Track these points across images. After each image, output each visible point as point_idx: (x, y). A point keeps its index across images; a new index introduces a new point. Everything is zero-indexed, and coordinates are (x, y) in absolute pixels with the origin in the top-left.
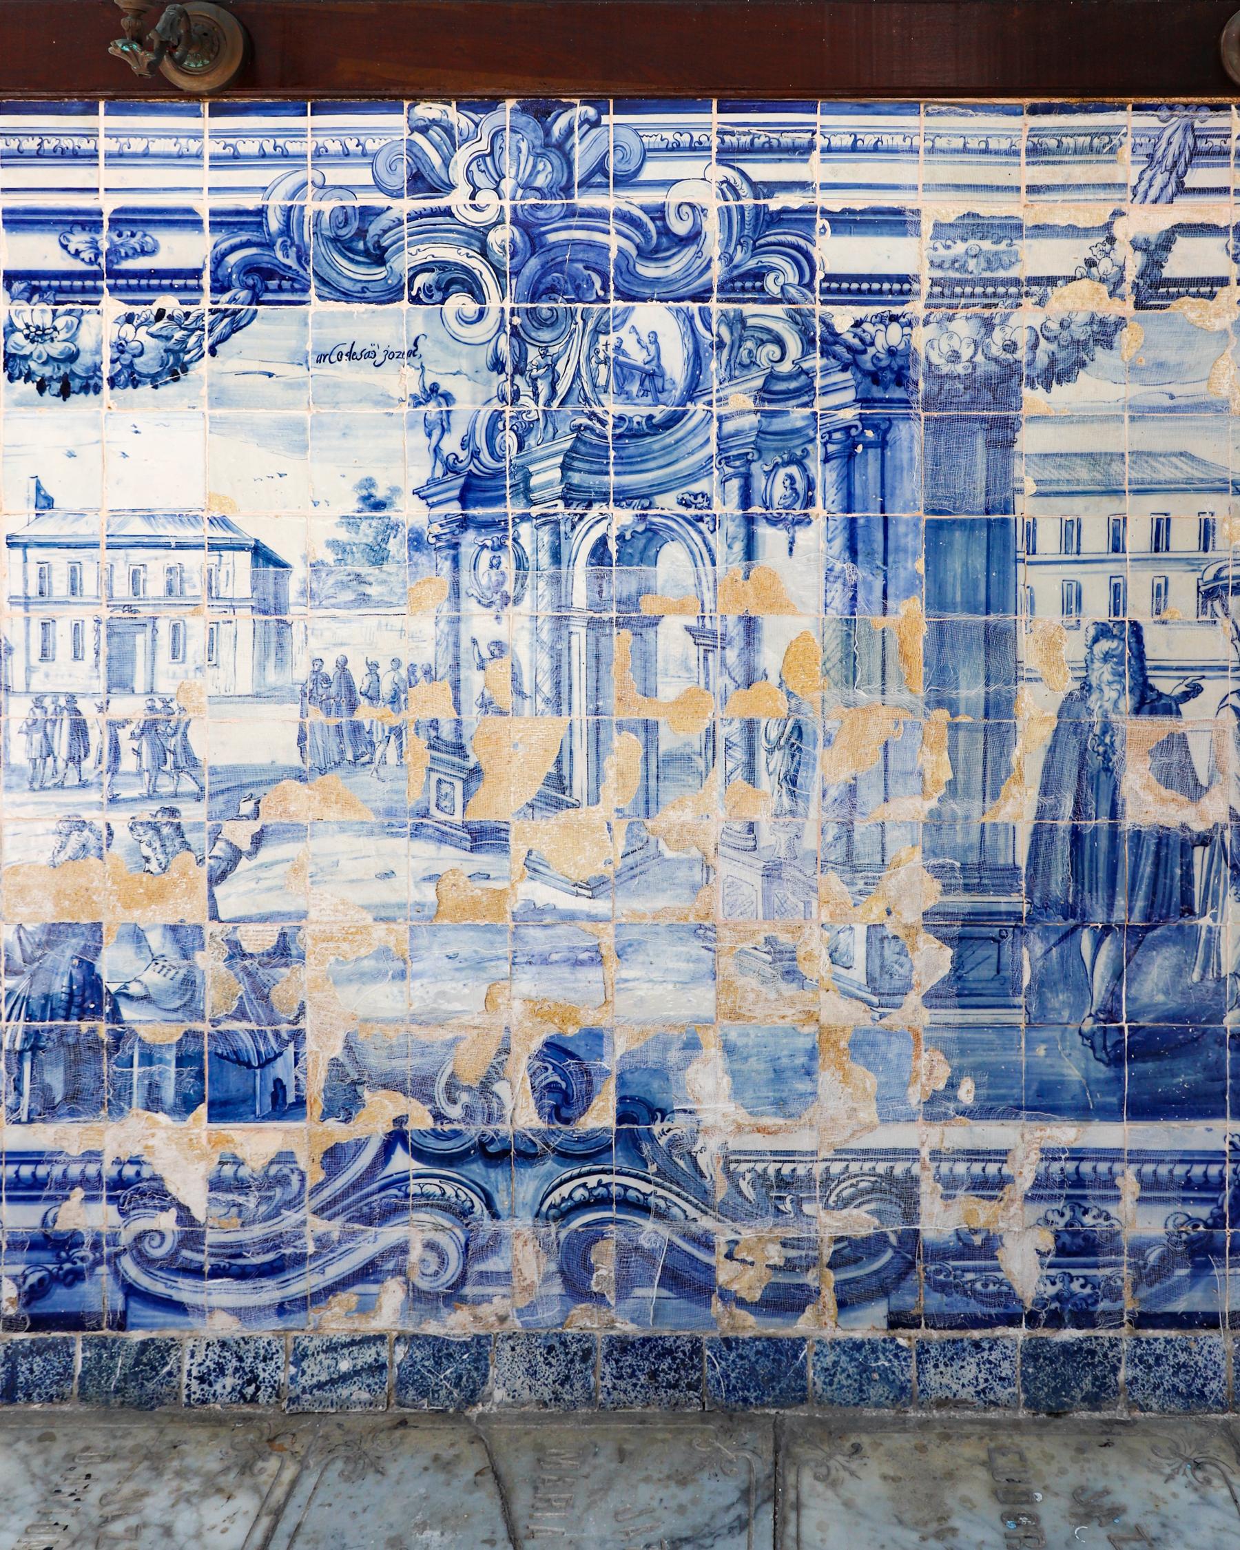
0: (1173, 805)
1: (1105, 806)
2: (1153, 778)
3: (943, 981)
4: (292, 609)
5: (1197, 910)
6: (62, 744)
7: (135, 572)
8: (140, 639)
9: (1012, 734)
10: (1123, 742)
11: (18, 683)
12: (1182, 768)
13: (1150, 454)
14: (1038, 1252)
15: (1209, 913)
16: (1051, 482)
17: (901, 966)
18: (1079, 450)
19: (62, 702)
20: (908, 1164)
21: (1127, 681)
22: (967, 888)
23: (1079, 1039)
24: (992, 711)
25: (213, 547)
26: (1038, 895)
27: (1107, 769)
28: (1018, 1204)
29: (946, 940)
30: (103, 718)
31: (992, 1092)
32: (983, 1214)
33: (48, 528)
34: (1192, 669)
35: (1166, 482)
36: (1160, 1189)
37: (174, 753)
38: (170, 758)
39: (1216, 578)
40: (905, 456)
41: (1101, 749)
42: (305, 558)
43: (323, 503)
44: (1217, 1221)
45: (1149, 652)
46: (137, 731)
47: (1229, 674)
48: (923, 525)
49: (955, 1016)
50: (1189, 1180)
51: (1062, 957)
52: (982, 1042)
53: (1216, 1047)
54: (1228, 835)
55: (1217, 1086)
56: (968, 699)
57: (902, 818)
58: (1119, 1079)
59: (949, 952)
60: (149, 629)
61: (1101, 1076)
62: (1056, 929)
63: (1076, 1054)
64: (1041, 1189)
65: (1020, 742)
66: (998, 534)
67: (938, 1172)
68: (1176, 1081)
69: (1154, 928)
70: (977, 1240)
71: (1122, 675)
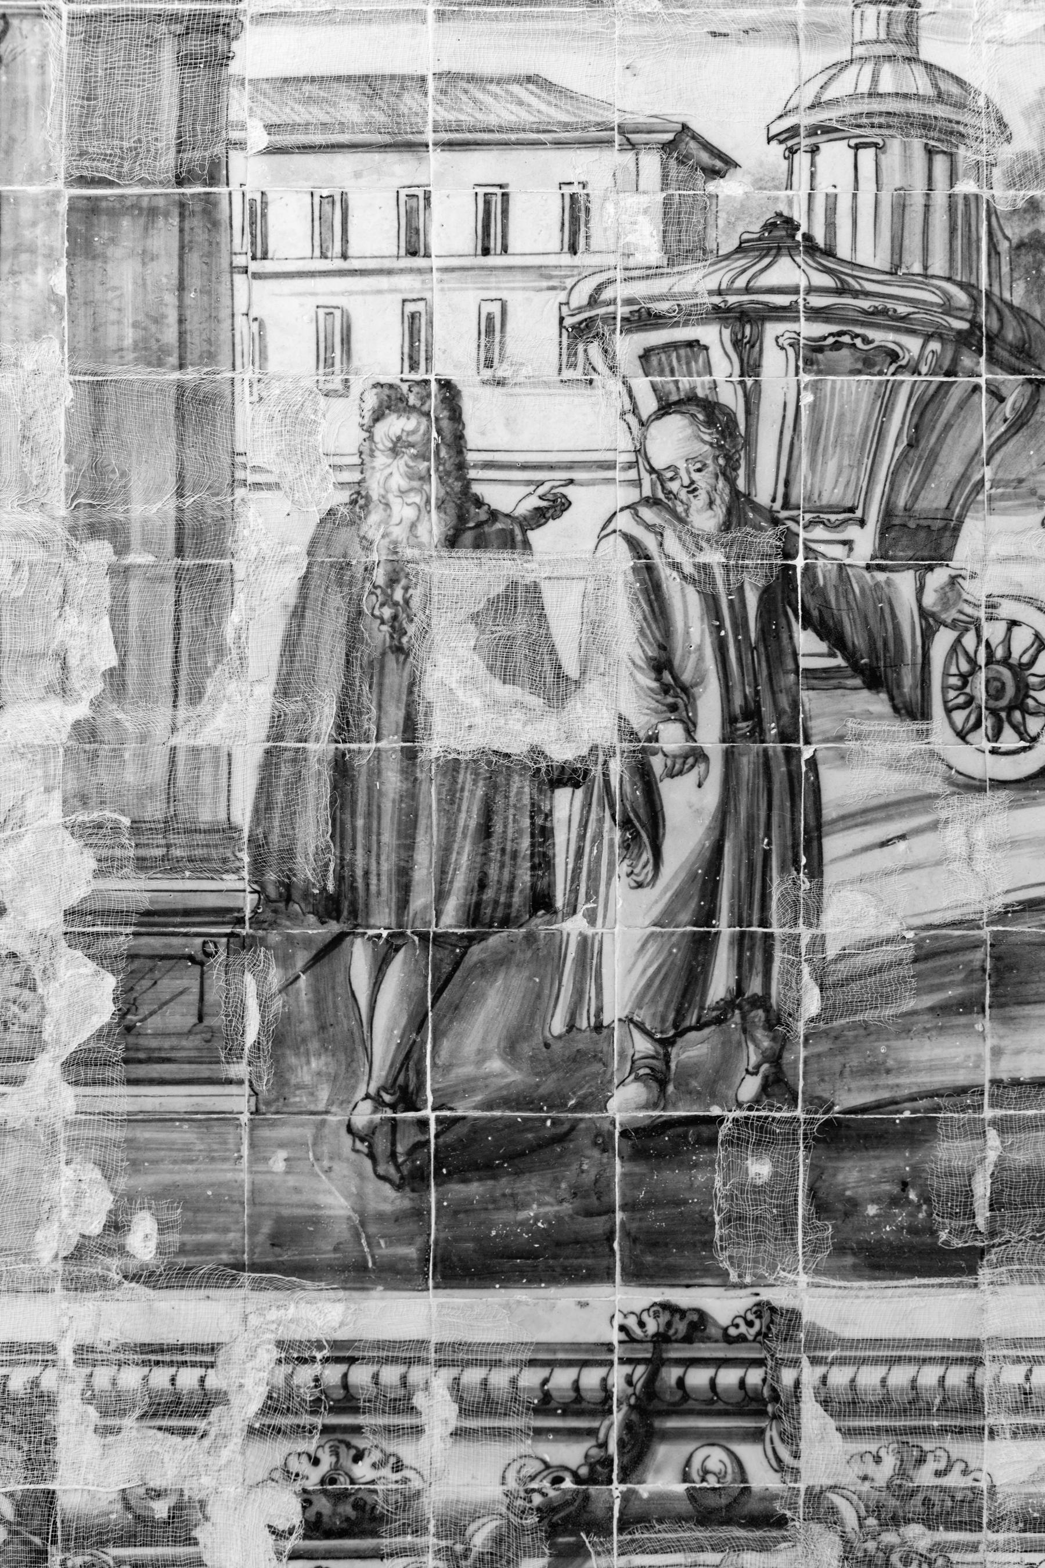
0: (518, 714)
1: (395, 715)
2: (482, 665)
3: (99, 1035)
5: (559, 902)
9: (225, 588)
10: (427, 598)
12: (533, 647)
13: (472, 78)
14: (273, 1531)
15: (582, 908)
16: (294, 127)
17: (24, 1008)
18: (343, 71)
20: (34, 1371)
21: (434, 488)
22: (142, 864)
23: (347, 1140)
24: (188, 542)
26: (271, 876)
27: (399, 650)
28: (237, 1440)
29: (101, 959)
31: (187, 1238)
32: (167, 1461)
34: (551, 467)
35: (501, 129)
36: (492, 1413)
39: (593, 301)
40: (32, 83)
41: (387, 612)
44: (598, 1471)
45: (473, 437)
47: (618, 475)
48: (63, 206)
49: (122, 1099)
50: (547, 1397)
51: (316, 991)
52: (171, 1146)
53: (596, 1153)
54: (616, 767)
55: (598, 1225)
56: (146, 521)
57: (28, 738)
58: (419, 1214)
59: (110, 982)
61: (387, 1208)
62: (308, 941)
63: (341, 1169)
64: (278, 1413)
65: (240, 598)
66: (195, 199)
67: (89, 1385)
68: (522, 1215)
69: (483, 937)
70: (161, 1509)
71: (425, 478)
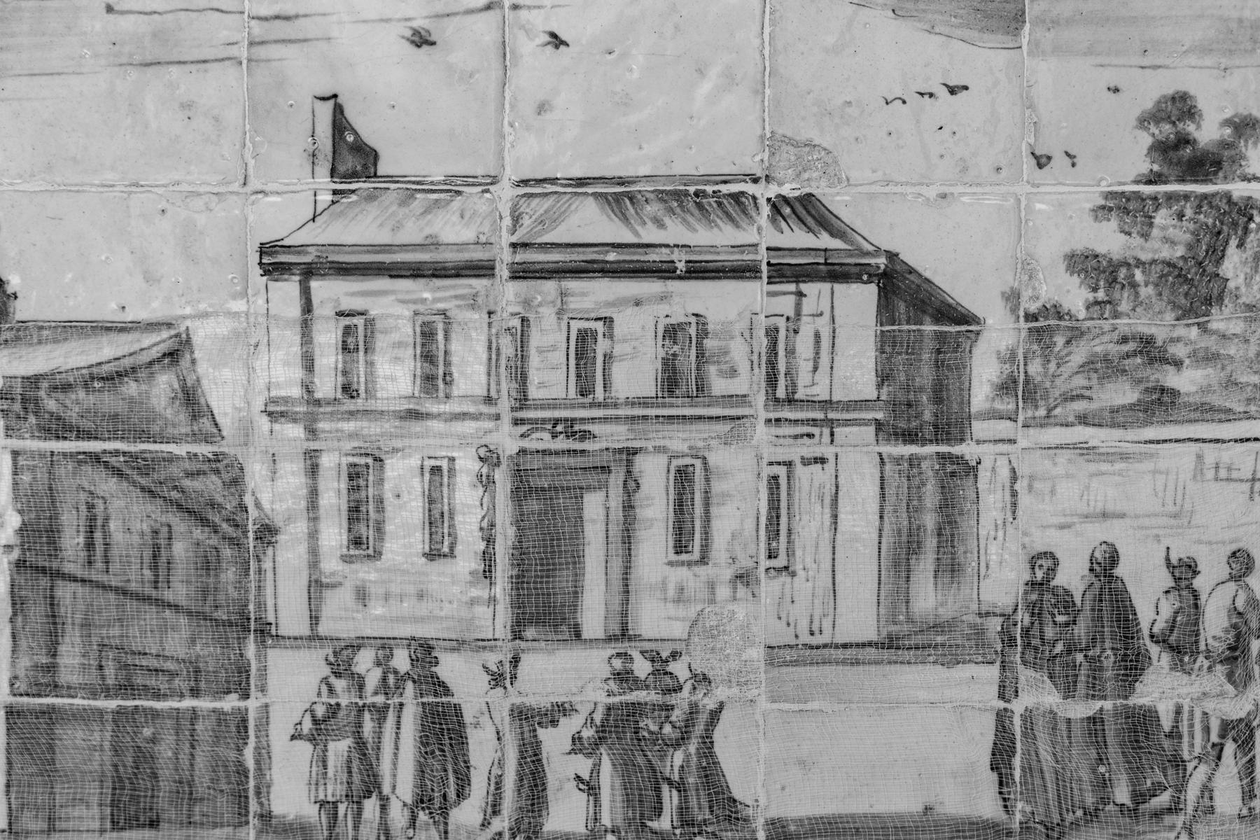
4: (980, 428)
6: (401, 769)
7: (585, 338)
8: (593, 505)
11: (292, 620)
19: (401, 661)
25: (779, 273)
30: (502, 702)
33: (363, 227)
37: (681, 787)
38: (670, 799)
42: (1012, 298)
43: (1059, 161)
46: (588, 733)
60: (616, 479)
